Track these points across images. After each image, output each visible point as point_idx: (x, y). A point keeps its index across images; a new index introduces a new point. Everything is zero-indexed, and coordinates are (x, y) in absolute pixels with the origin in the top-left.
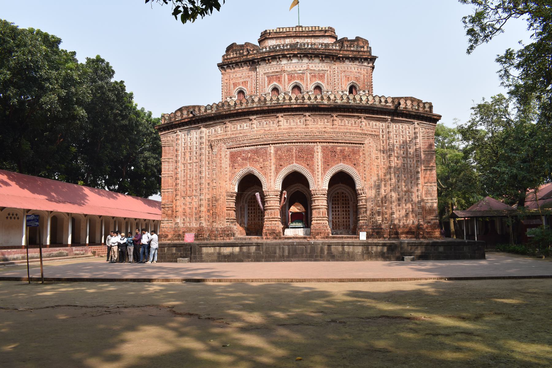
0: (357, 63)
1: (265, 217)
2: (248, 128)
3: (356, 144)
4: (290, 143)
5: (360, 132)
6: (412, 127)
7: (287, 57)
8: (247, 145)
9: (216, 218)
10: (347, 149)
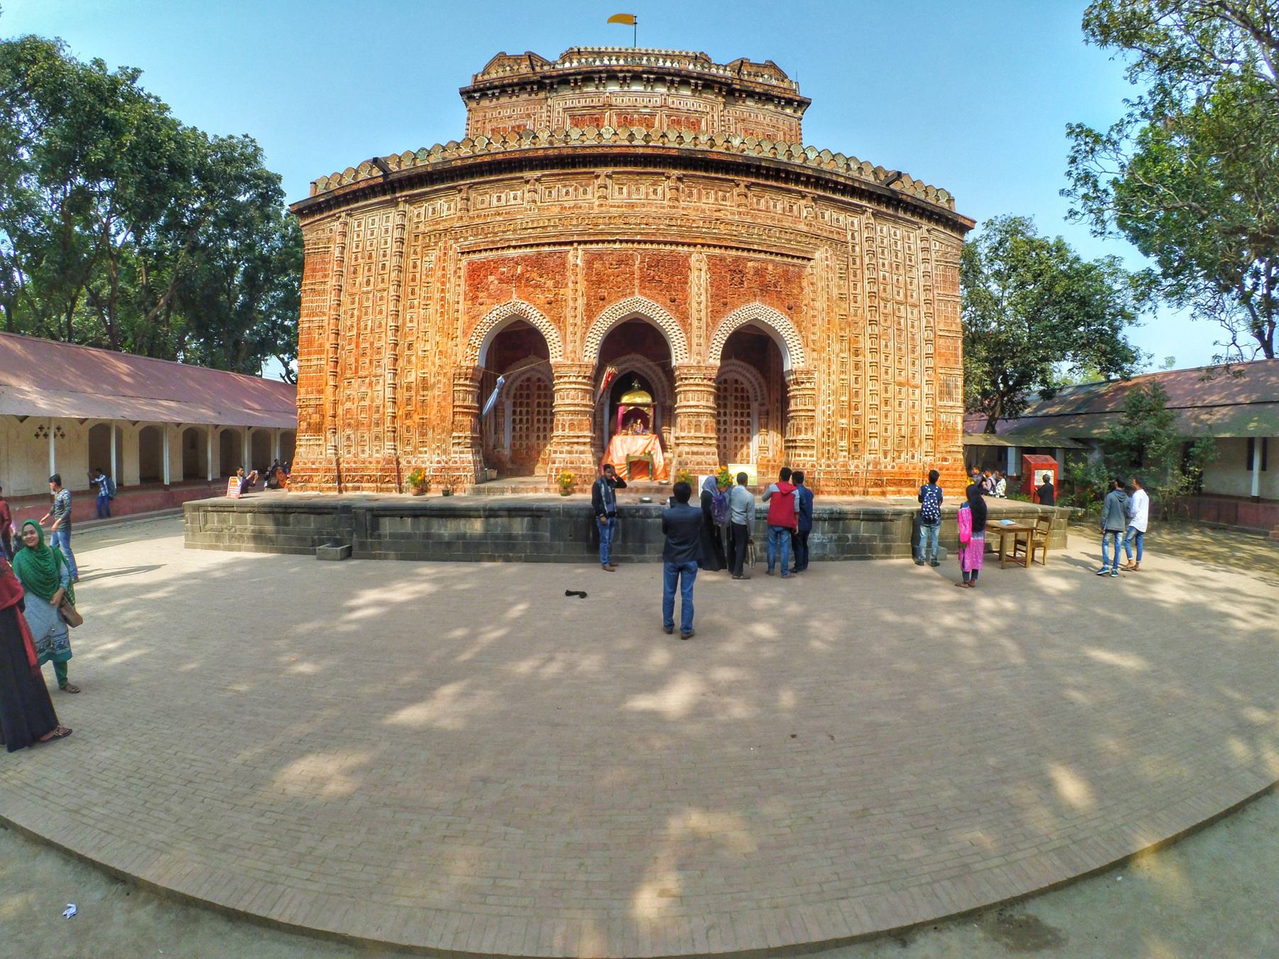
0: (771, 107)
1: (555, 433)
2: (519, 201)
3: (793, 257)
4: (627, 242)
5: (805, 229)
6: (915, 235)
7: (617, 78)
8: (514, 243)
9: (424, 434)
10: (770, 267)
